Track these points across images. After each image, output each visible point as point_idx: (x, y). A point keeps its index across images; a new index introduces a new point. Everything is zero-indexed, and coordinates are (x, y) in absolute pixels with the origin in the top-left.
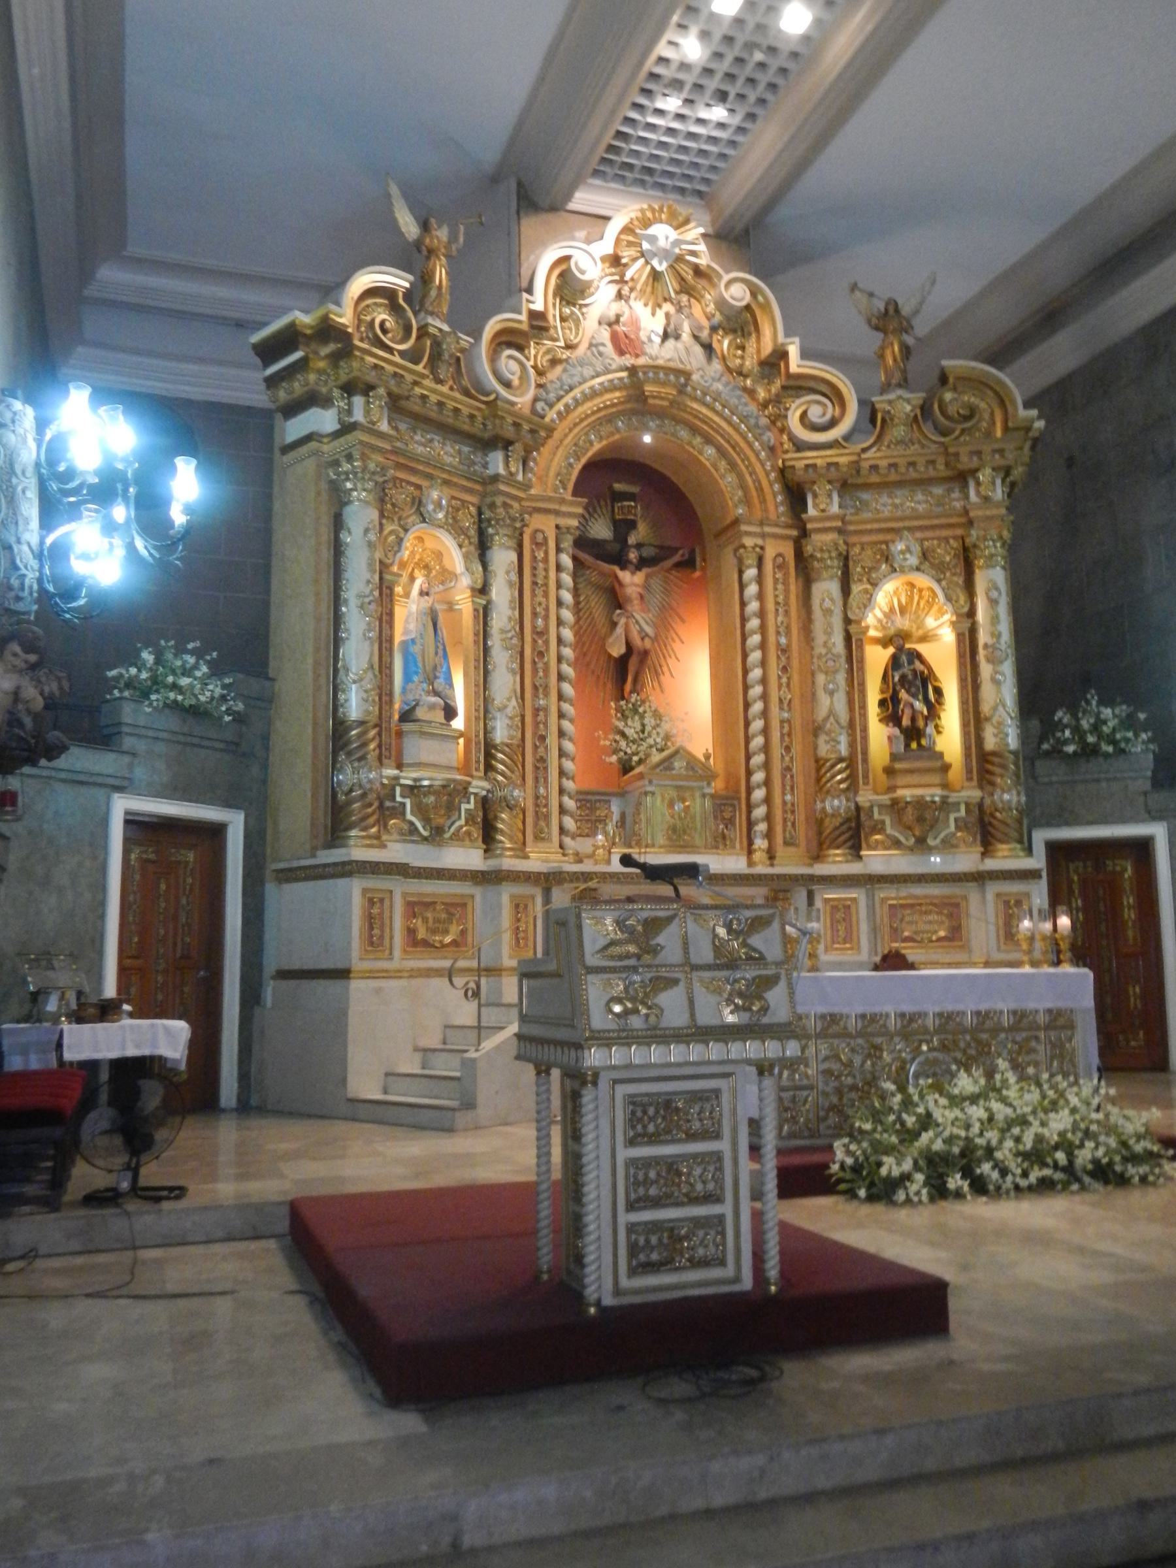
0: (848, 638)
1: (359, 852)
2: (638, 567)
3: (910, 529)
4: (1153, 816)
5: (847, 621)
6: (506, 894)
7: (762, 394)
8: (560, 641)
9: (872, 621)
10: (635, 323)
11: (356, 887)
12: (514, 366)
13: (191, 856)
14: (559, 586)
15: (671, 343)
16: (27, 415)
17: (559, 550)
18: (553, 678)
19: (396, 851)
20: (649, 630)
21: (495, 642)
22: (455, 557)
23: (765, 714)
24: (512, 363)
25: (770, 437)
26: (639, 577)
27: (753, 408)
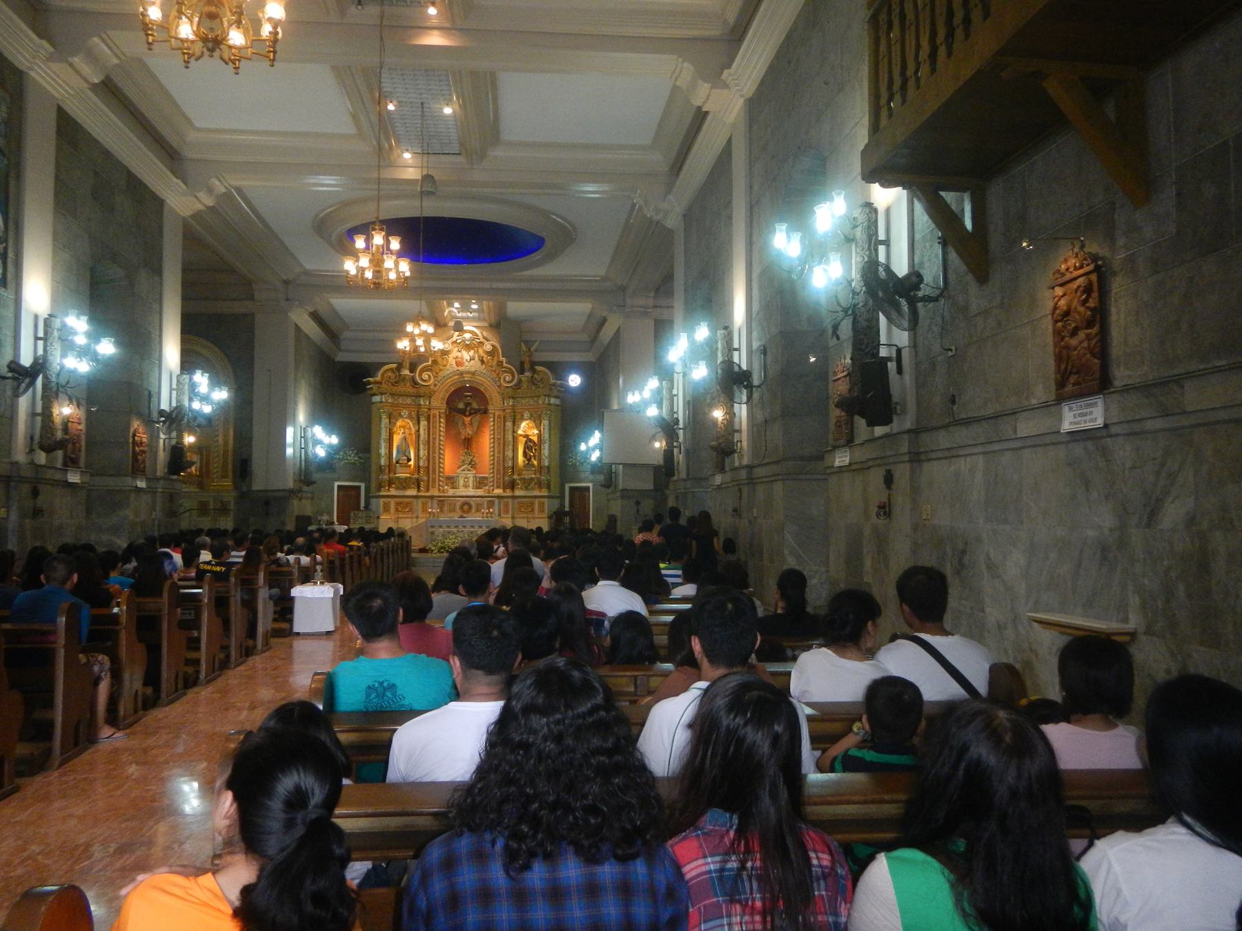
0: (513, 436)
1: (382, 493)
2: (470, 415)
3: (528, 409)
4: (591, 482)
5: (514, 432)
6: (420, 501)
7: (497, 372)
8: (440, 440)
9: (520, 432)
10: (462, 358)
11: (382, 501)
12: (427, 376)
13: (353, 493)
14: (440, 426)
15: (472, 361)
16: (309, 429)
17: (440, 417)
18: (437, 449)
19: (393, 492)
20: (470, 433)
21: (421, 443)
22: (411, 424)
23: (494, 455)
24: (425, 376)
25: (498, 383)
26: (469, 418)
27: (495, 375)
